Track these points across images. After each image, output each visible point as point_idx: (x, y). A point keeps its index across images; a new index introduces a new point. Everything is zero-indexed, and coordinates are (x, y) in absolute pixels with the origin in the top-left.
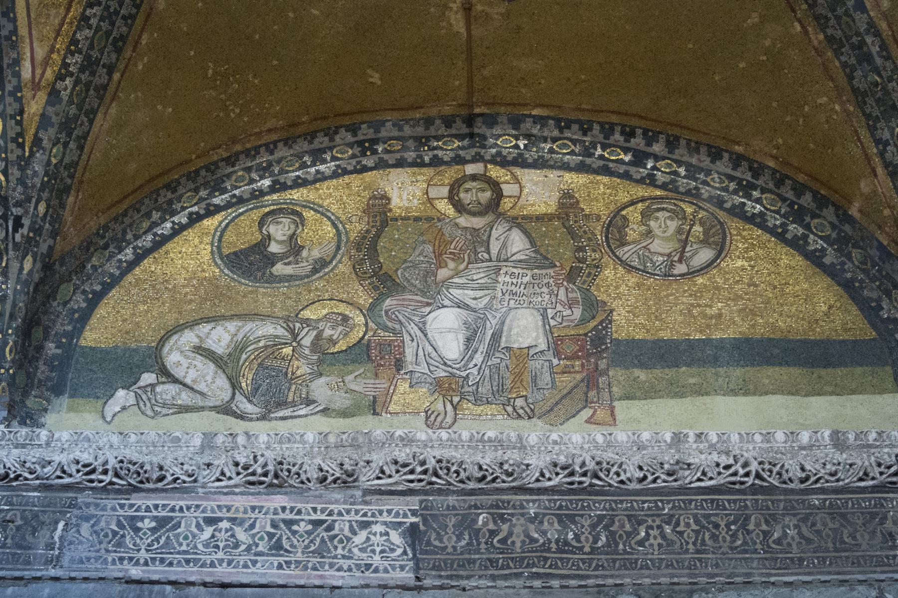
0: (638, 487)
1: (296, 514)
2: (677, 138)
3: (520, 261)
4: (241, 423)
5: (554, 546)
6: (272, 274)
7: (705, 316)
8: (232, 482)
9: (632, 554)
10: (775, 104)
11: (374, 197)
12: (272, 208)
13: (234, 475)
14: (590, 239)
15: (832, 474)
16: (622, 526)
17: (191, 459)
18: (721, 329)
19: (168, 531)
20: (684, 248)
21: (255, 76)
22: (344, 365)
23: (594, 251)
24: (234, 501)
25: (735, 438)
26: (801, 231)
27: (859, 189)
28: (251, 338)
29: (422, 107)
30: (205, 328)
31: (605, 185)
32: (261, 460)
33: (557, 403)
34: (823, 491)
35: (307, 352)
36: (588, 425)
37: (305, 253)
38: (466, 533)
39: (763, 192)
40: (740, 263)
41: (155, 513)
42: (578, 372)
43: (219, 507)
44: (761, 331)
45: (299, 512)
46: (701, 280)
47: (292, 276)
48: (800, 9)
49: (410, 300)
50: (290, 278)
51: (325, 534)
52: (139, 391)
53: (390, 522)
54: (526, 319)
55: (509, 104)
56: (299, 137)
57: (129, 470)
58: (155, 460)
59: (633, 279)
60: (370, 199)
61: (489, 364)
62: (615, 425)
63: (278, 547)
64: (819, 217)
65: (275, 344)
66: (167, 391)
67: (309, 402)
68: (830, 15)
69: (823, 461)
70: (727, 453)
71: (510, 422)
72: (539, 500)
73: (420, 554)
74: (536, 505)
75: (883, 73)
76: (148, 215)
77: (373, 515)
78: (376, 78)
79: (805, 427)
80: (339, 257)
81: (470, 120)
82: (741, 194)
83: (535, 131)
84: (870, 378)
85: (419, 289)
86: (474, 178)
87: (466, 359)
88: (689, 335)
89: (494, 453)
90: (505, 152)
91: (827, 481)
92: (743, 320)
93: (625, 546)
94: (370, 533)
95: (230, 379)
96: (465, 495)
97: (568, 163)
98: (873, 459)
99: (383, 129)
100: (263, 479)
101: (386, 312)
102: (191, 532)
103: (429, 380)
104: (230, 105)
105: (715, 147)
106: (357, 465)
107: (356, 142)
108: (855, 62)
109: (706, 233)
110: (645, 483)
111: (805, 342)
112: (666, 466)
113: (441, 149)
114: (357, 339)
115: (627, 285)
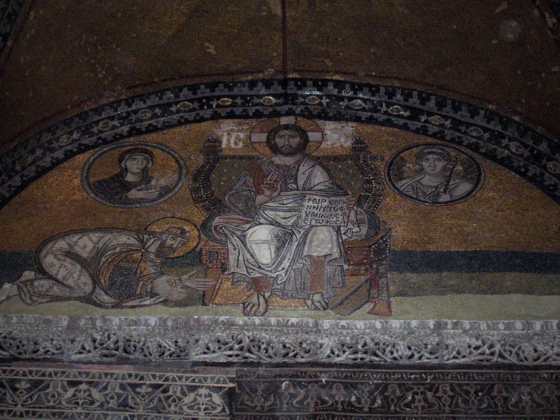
0: (407, 362)
1: (140, 380)
2: (445, 99)
3: (321, 190)
5: (340, 406)
6: (126, 197)
8: (90, 355)
9: (402, 413)
11: (209, 141)
12: (129, 148)
14: (375, 175)
16: (394, 392)
17: (59, 336)
19: (39, 391)
21: (117, 46)
22: (181, 267)
23: (378, 183)
24: (92, 368)
25: (483, 326)
26: (538, 171)
28: (110, 246)
32: (113, 338)
34: (551, 367)
35: (152, 256)
37: (153, 182)
38: (272, 396)
41: (30, 377)
42: (364, 275)
43: (80, 373)
45: (142, 378)
47: (142, 199)
50: (141, 201)
51: (162, 395)
52: (21, 285)
53: (213, 387)
54: (324, 234)
56: (152, 93)
57: (11, 344)
60: (206, 142)
61: (294, 267)
62: (390, 315)
63: (124, 405)
64: (553, 160)
65: (129, 250)
66: (43, 284)
67: (153, 295)
69: (551, 344)
73: (236, 411)
74: (327, 375)
76: (33, 151)
77: (200, 381)
79: (538, 318)
80: (180, 185)
81: (284, 83)
82: (493, 142)
86: (287, 127)
87: (276, 263)
90: (311, 108)
93: (395, 406)
94: (197, 394)
99: (217, 89)
100: (114, 352)
101: (216, 227)
102: (57, 392)
106: (188, 342)
107: (196, 99)
109: (465, 170)
112: (429, 347)
114: (192, 248)
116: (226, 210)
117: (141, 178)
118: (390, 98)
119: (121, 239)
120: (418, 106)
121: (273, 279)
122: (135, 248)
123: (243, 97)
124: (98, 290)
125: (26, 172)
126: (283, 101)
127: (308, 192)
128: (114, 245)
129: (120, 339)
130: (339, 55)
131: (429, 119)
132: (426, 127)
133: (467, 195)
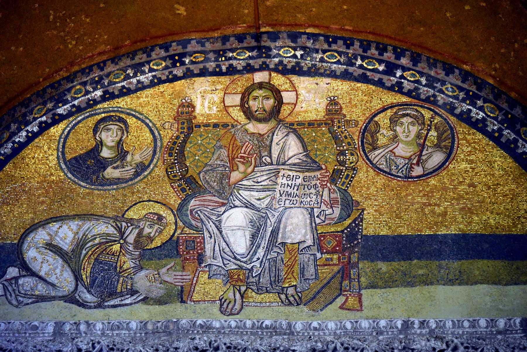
2: (419, 55)
4: (83, 310)
6: (104, 177)
7: (433, 212)
11: (182, 105)
12: (103, 115)
14: (349, 144)
17: (46, 346)
20: (421, 151)
21: (87, 17)
22: (159, 259)
23: (352, 154)
25: (449, 324)
26: (513, 136)
29: (219, 29)
30: (54, 226)
31: (363, 92)
33: (318, 292)
36: (341, 311)
37: (129, 158)
39: (484, 103)
40: (464, 165)
42: (336, 265)
46: (433, 182)
47: (119, 179)
49: (210, 201)
50: (118, 181)
54: (298, 217)
55: (287, 25)
56: (123, 55)
59: (381, 180)
60: (179, 106)
61: (268, 257)
65: (108, 241)
66: (27, 282)
67: (133, 292)
69: (512, 346)
70: (441, 339)
71: (282, 309)
76: (8, 127)
78: (182, 10)
80: (155, 160)
81: (257, 37)
82: (468, 102)
83: (309, 44)
85: (216, 191)
86: (260, 86)
87: (251, 253)
88: (421, 231)
89: (269, 340)
90: (285, 61)
92: (463, 217)
95: (73, 272)
97: (335, 71)
99: (189, 46)
101: (191, 211)
104: (69, 39)
105: (448, 64)
109: (439, 137)
111: (509, 237)
113: (235, 59)
115: (375, 186)
116: (202, 190)
117: (117, 153)
118: (365, 51)
119: (99, 229)
120: (392, 59)
121: (248, 271)
123: (215, 52)
124: (81, 288)
126: (257, 54)
127: (283, 167)
128: (95, 235)
129: (104, 348)
130: (311, 11)
131: (404, 74)
133: (440, 167)
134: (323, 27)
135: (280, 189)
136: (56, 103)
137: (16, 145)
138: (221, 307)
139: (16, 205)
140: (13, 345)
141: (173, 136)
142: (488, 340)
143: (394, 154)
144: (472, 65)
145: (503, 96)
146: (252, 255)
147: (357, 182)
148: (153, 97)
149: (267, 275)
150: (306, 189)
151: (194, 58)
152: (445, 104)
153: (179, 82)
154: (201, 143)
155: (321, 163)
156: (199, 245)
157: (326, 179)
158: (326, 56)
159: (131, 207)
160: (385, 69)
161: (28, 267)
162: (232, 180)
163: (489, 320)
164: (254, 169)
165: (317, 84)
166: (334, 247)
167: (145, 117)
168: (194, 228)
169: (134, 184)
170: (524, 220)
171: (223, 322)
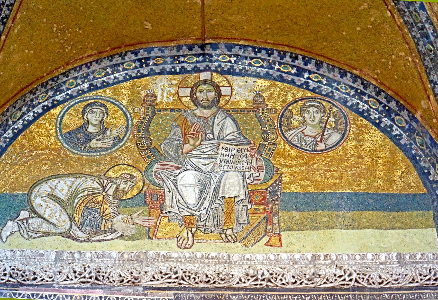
0: (292, 286)
2: (322, 63)
4: (76, 243)
6: (90, 146)
7: (332, 176)
8: (73, 282)
10: (376, 51)
11: (147, 95)
12: (89, 101)
13: (73, 278)
14: (270, 126)
15: (395, 280)
17: (50, 269)
18: (342, 186)
20: (324, 132)
22: (132, 207)
23: (273, 133)
24: (74, 292)
25: (345, 258)
26: (389, 122)
27: (421, 105)
31: (280, 89)
32: (88, 270)
33: (250, 233)
34: (391, 289)
35: (111, 199)
37: (108, 133)
40: (354, 143)
42: (262, 213)
43: (66, 296)
44: (363, 189)
46: (332, 154)
47: (101, 148)
48: (390, 5)
50: (101, 149)
52: (20, 223)
54: (234, 179)
55: (225, 38)
56: (105, 58)
57: (17, 274)
58: (32, 269)
59: (294, 153)
60: (145, 96)
61: (212, 207)
64: (399, 115)
66: (35, 222)
67: (113, 231)
68: (406, 10)
69: (391, 273)
70: (341, 268)
71: (223, 244)
72: (239, 294)
74: (237, 297)
75: (434, 45)
76: (20, 109)
78: (149, 26)
80: (128, 135)
81: (202, 47)
83: (241, 53)
84: (421, 218)
85: (173, 158)
86: (205, 82)
89: (214, 267)
90: (223, 65)
91: (393, 284)
96: (198, 291)
97: (259, 73)
98: (417, 272)
99: (152, 52)
100: (89, 280)
103: (179, 218)
105: (343, 70)
106: (140, 273)
108: (419, 36)
109: (336, 122)
110: (296, 285)
111: (387, 195)
112: (308, 276)
113: (186, 62)
115: (290, 157)
116: (162, 157)
117: (100, 129)
118: (282, 59)
119: (87, 184)
120: (302, 66)
122: (98, 191)
125: (15, 126)
127: (222, 141)
128: (84, 189)
129: (92, 271)
130: (243, 28)
132: (308, 82)
134: (251, 40)
135: (220, 157)
136: (55, 92)
137: (26, 122)
138: (178, 243)
139: (26, 166)
140: (27, 267)
141: (141, 117)
142: (373, 269)
143: (304, 133)
144: (360, 70)
145: (382, 93)
146: (200, 205)
147: (277, 153)
148: (126, 88)
149: (211, 220)
150: (239, 158)
151: (156, 61)
152: (340, 98)
153: (145, 78)
154: (161, 123)
155: (250, 139)
156: (161, 197)
157: (254, 151)
158: (253, 62)
159: (111, 168)
160: (296, 72)
161: (36, 211)
162: (185, 150)
163: (374, 254)
164: (201, 143)
165: (246, 82)
166: (261, 201)
167: (120, 103)
168: (157, 185)
169: (112, 152)
170: (398, 183)
171: (180, 254)
